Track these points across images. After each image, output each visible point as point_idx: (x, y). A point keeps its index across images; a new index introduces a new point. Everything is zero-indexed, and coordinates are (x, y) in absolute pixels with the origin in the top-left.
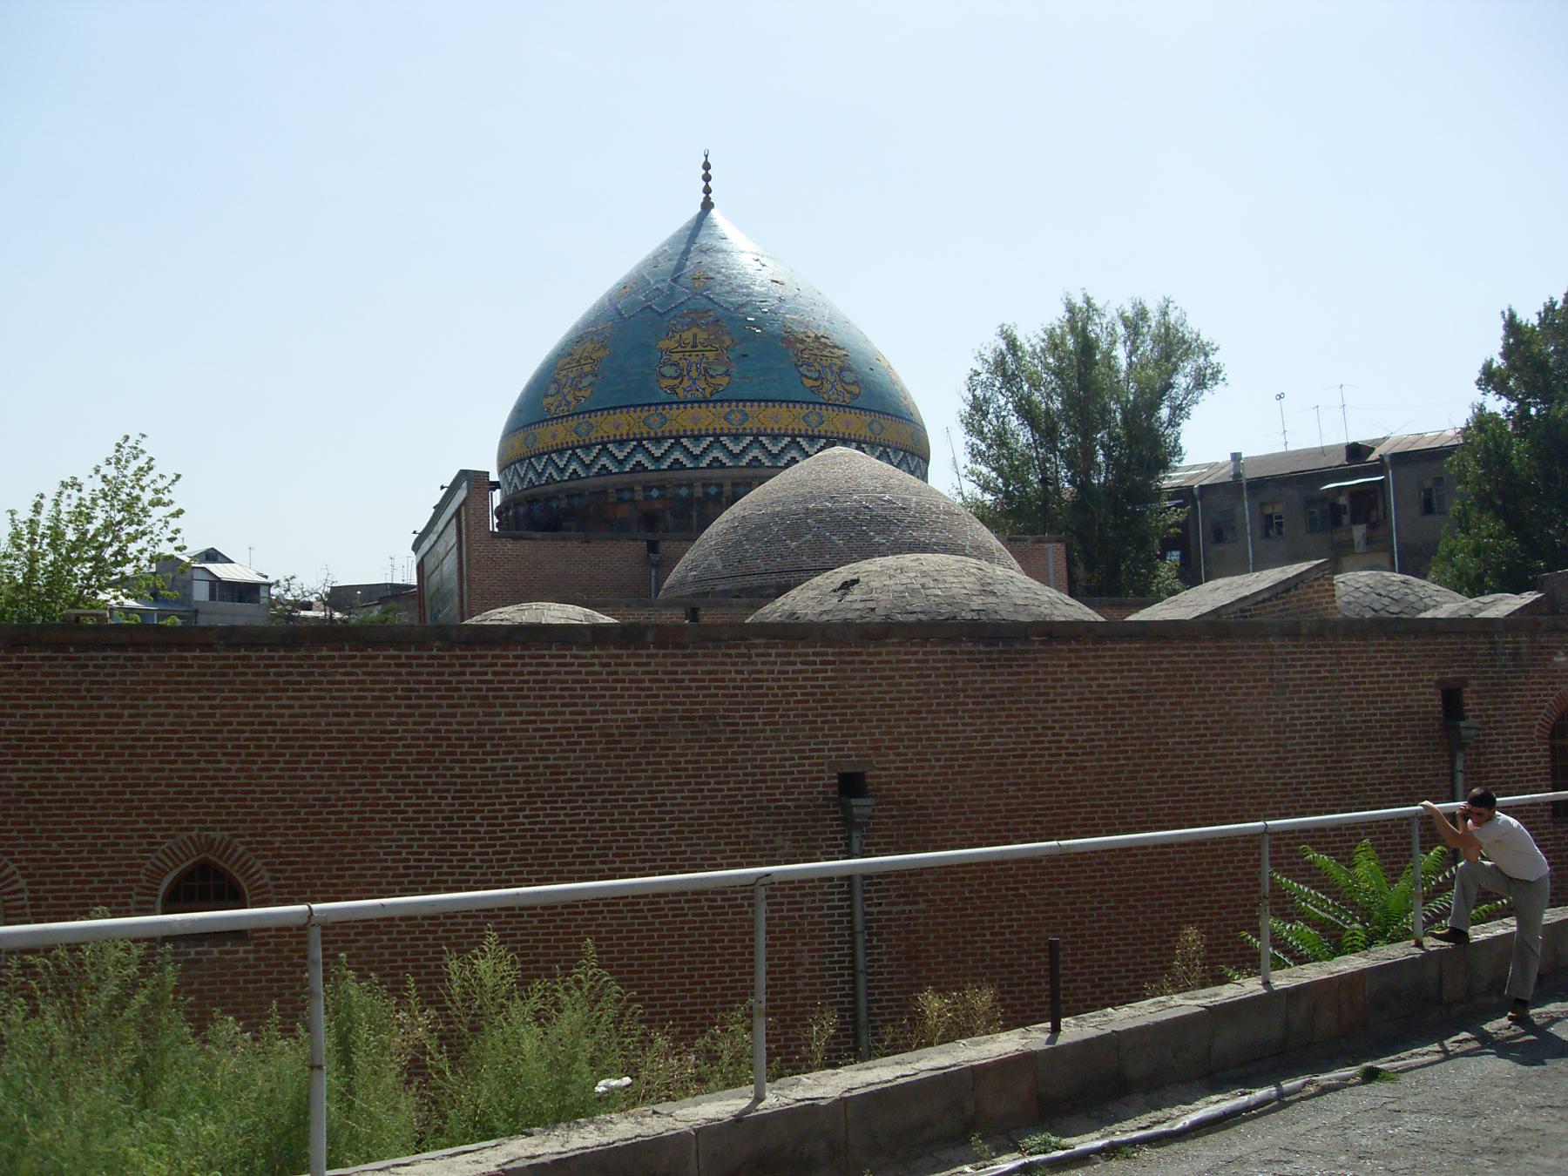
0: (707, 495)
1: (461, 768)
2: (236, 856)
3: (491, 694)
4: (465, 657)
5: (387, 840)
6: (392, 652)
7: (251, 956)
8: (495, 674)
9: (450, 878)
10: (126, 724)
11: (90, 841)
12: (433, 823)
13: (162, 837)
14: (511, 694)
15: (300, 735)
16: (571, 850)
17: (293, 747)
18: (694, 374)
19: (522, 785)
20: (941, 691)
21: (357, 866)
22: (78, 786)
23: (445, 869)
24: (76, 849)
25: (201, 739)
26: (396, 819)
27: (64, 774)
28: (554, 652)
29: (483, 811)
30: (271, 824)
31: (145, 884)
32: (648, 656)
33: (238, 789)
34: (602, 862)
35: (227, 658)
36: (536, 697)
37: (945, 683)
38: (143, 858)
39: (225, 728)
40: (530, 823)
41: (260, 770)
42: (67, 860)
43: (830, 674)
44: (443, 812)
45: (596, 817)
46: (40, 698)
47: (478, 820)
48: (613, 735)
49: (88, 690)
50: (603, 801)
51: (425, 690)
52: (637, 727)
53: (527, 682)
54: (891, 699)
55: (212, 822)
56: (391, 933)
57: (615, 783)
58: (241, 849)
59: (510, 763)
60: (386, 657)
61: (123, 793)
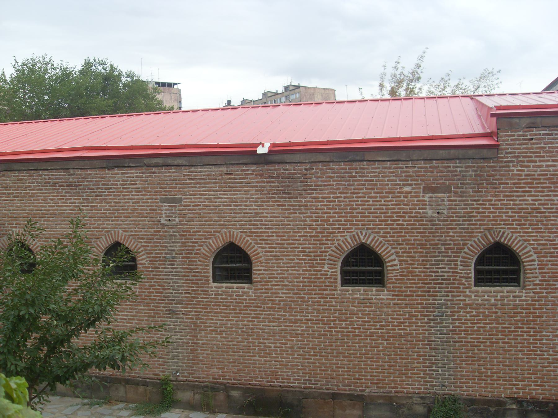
46: (543, 157)
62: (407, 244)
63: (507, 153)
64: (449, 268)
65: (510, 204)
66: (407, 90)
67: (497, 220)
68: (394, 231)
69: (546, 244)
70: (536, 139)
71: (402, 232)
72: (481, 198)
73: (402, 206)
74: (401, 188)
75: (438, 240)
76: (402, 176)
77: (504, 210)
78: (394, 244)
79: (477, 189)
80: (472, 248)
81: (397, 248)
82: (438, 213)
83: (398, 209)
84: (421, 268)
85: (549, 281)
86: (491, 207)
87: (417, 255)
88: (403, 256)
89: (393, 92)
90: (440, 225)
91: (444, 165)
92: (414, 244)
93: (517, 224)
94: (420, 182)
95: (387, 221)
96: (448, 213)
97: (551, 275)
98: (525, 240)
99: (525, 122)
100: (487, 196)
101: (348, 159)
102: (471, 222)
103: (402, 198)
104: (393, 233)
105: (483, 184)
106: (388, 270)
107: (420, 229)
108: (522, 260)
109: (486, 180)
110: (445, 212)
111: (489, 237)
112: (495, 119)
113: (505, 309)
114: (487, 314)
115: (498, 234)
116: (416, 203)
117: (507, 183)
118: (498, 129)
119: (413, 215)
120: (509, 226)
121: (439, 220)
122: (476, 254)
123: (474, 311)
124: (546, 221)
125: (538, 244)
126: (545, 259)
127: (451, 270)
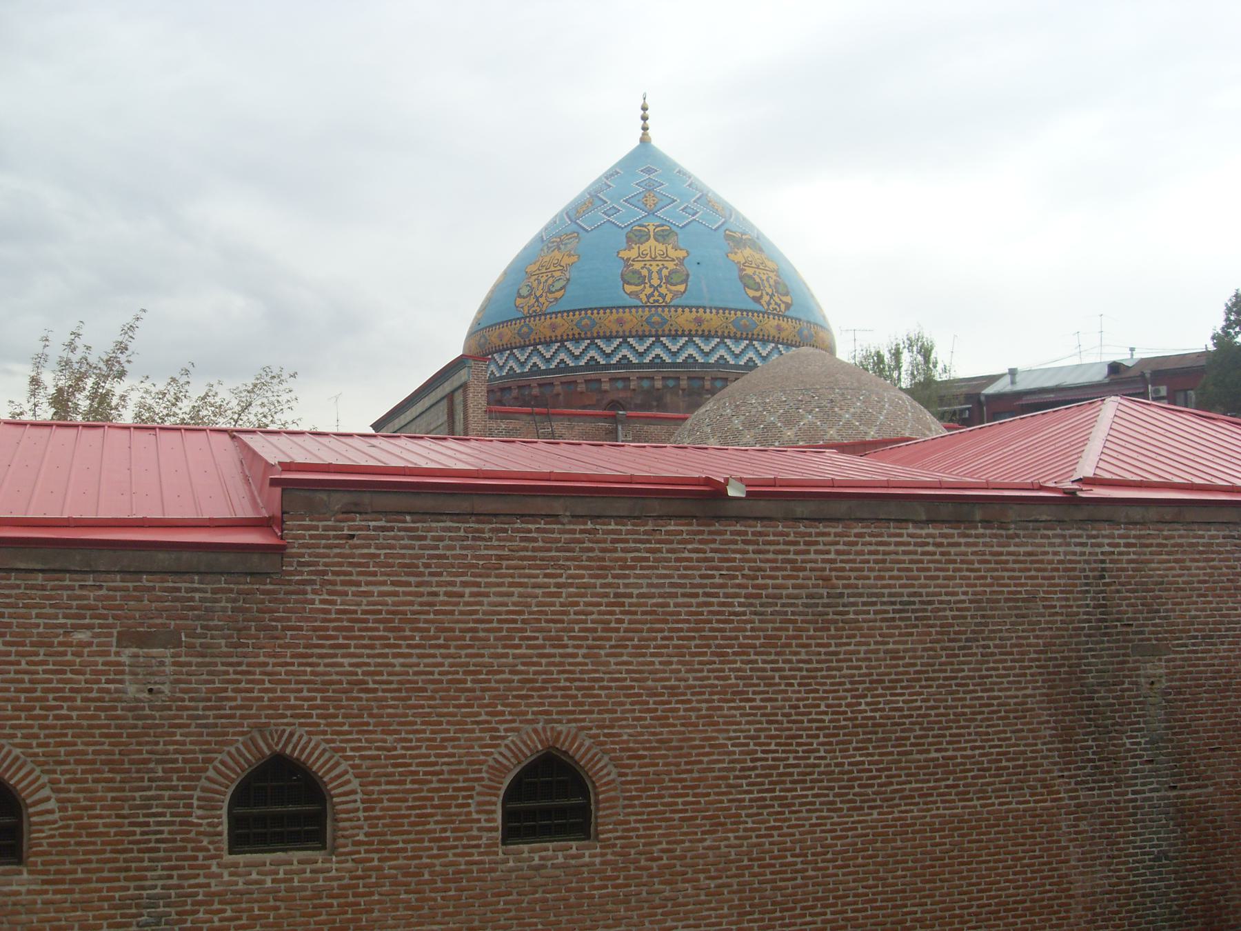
0: (665, 387)
1: (807, 653)
2: (583, 750)
3: (834, 574)
4: (810, 535)
5: (735, 731)
6: (738, 528)
7: (598, 860)
8: (838, 552)
9: (796, 770)
10: (467, 604)
11: (428, 735)
12: (779, 712)
13: (506, 730)
14: (853, 574)
15: (649, 617)
16: (908, 738)
17: (641, 631)
18: (655, 282)
19: (864, 671)
20: (1224, 575)
21: (705, 759)
22: (416, 673)
23: (791, 761)
24: (414, 744)
25: (547, 621)
26: (744, 708)
27: (402, 660)
28: (892, 530)
29: (827, 698)
30: (619, 715)
31: (486, 782)
32: (977, 536)
33: (586, 676)
34: (937, 751)
35: (573, 532)
36: (876, 578)
37: (1227, 567)
38: (484, 754)
39: (572, 609)
40: (872, 711)
41: (607, 655)
42: (404, 756)
43: (1132, 557)
44: (790, 699)
45: (932, 703)
46: (374, 574)
47: (823, 708)
48: (946, 617)
49: (427, 566)
50: (938, 687)
51: (772, 569)
52: (968, 609)
53: (868, 562)
54: (1184, 583)
55: (559, 713)
56: (737, 830)
57: (949, 668)
58: (587, 743)
59: (852, 648)
60: (732, 533)
61: (465, 681)
62: (77, 762)
63: (300, 564)
64: (173, 815)
65: (305, 673)
66: (92, 398)
67: (276, 708)
68: (47, 732)
69: (378, 757)
70: (360, 537)
71: (66, 735)
72: (246, 660)
73: (69, 676)
74: (66, 634)
75: (149, 752)
77: (293, 686)
78: (46, 763)
80: (223, 768)
81: (54, 772)
82: (150, 691)
83: (59, 681)
84: (109, 816)
85: (385, 834)
86: (266, 678)
87: (100, 786)
88: (68, 791)
89: (61, 401)
90: (154, 718)
91: (166, 585)
92: (93, 762)
93: (318, 716)
94: (111, 621)
95: (34, 708)
96: (173, 691)
97: (387, 821)
98: (336, 750)
99: (339, 500)
100: (257, 656)
102: (222, 712)
103: (69, 657)
104: (46, 736)
105: (249, 628)
106: (31, 824)
107: (108, 726)
108: (329, 791)
110: (166, 688)
111: (262, 744)
112: (278, 491)
113: (294, 899)
114: (257, 912)
115: (280, 737)
116: (100, 667)
117: (300, 628)
118: (283, 513)
119: (94, 695)
120: (302, 720)
121: (151, 708)
122: (232, 781)
123: (228, 907)
124: (378, 708)
125: (362, 758)
126: (377, 788)
127: (178, 819)
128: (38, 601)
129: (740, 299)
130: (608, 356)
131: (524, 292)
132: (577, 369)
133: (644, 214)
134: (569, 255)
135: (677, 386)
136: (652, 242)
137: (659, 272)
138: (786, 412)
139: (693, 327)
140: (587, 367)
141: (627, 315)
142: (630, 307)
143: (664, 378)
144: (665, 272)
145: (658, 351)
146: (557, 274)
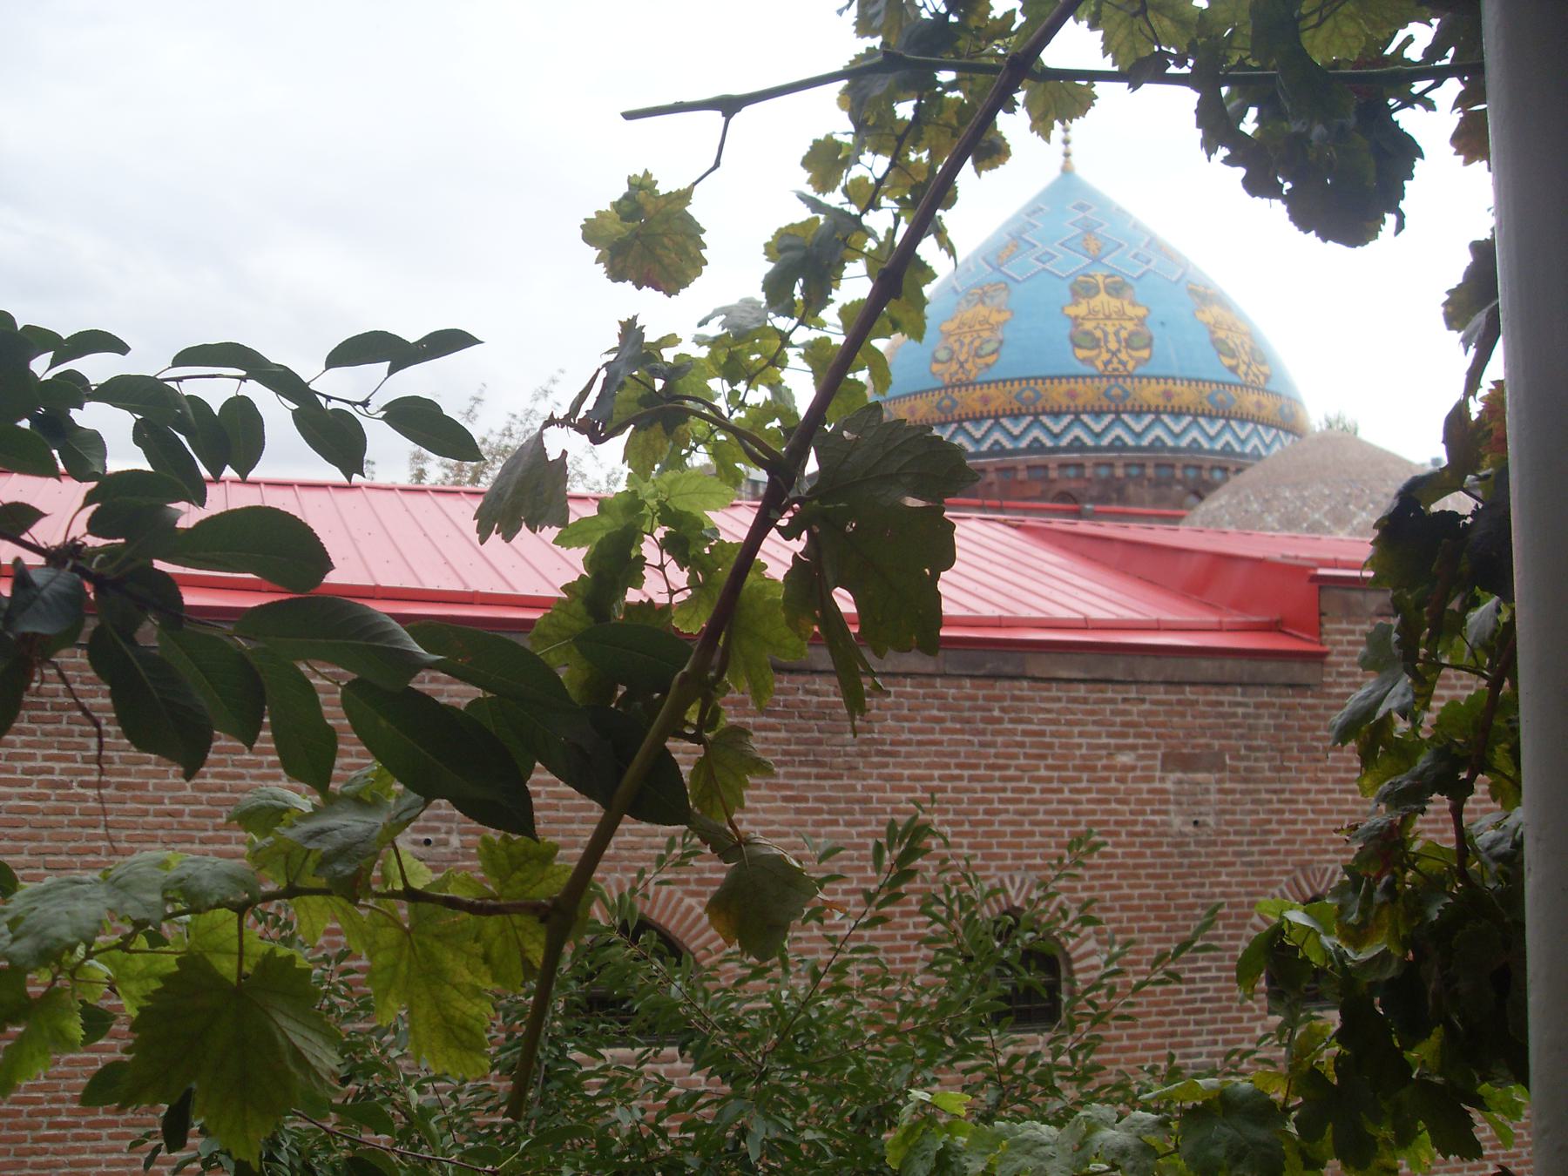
0: (1128, 476)
18: (1113, 345)
62: (1123, 908)
63: (1340, 674)
64: (1219, 969)
65: (1346, 801)
72: (1289, 786)
73: (1114, 806)
74: (1110, 756)
76: (1112, 724)
79: (1278, 763)
82: (1196, 823)
86: (1309, 807)
87: (1147, 936)
90: (1198, 854)
92: (1139, 908)
94: (1154, 740)
96: (1218, 824)
100: (1299, 781)
101: (982, 672)
103: (1113, 784)
105: (1290, 749)
109: (1299, 739)
110: (1211, 820)
115: (1323, 876)
116: (1145, 796)
119: (1139, 828)
121: (1198, 843)
127: (1224, 974)
128: (1080, 716)
129: (1215, 369)
130: (1056, 436)
131: (943, 355)
132: (1015, 452)
133: (1088, 261)
134: (999, 311)
135: (1142, 476)
136: (1103, 296)
137: (1117, 334)
138: (1333, 509)
139: (1161, 402)
140: (1029, 450)
141: (1079, 387)
142: (1084, 377)
143: (1127, 465)
144: (1124, 334)
145: (1118, 431)
146: (985, 335)
